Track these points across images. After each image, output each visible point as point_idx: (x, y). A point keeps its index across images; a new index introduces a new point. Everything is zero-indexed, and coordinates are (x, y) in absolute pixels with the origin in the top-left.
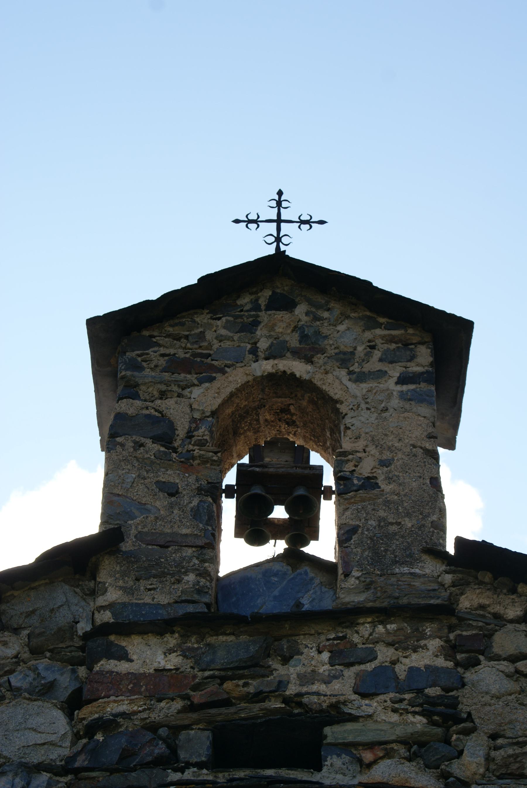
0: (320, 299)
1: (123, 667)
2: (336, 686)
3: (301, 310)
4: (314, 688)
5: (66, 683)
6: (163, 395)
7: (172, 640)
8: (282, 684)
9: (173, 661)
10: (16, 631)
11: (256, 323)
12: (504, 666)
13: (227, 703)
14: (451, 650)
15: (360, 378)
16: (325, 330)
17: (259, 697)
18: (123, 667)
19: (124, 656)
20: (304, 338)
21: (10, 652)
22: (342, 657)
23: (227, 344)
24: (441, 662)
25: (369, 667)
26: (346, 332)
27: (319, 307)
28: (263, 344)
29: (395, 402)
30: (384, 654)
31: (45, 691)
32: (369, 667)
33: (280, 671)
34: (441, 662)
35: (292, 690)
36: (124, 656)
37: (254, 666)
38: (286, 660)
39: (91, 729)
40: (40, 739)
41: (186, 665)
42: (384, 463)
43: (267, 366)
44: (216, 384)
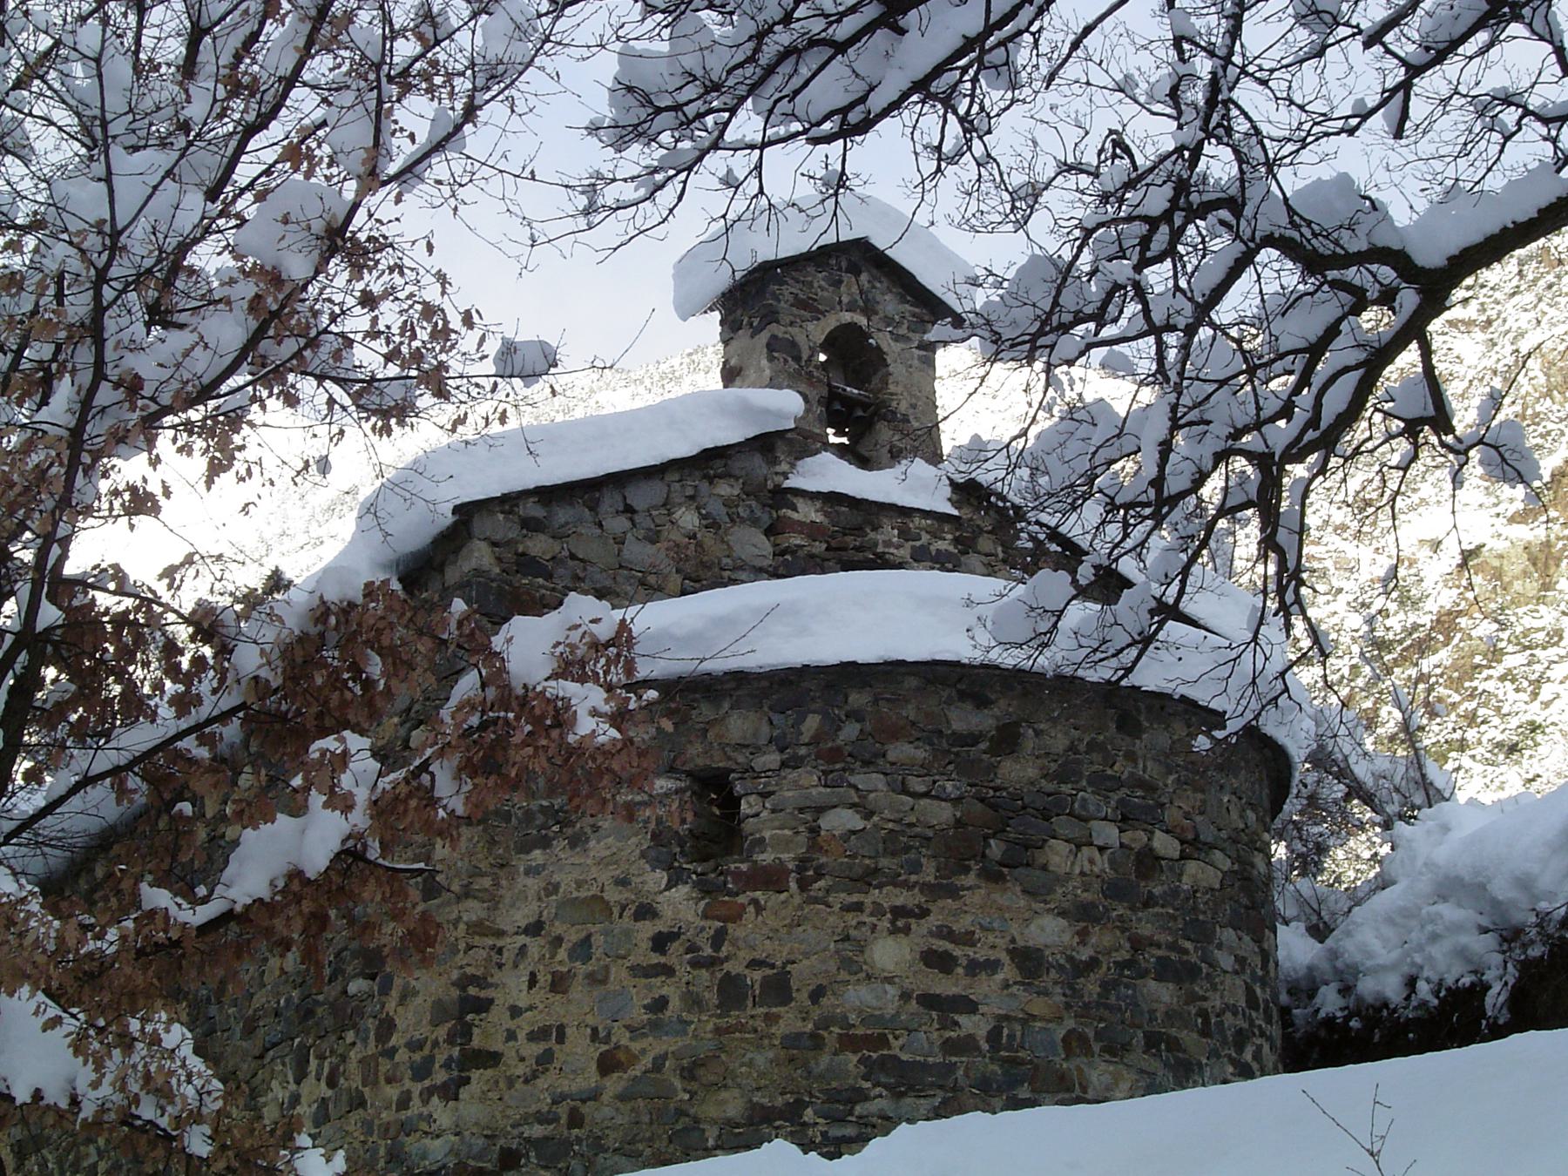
0: (875, 271)
1: (790, 513)
2: (902, 552)
3: (864, 277)
4: (892, 550)
5: (766, 520)
6: (791, 324)
7: (818, 504)
8: (876, 545)
9: (818, 518)
10: (737, 479)
11: (841, 282)
12: (983, 558)
13: (845, 549)
14: (956, 541)
15: (897, 338)
16: (879, 298)
17: (858, 549)
18: (795, 516)
19: (795, 509)
20: (866, 301)
21: (736, 492)
22: (905, 534)
23: (826, 294)
24: (951, 548)
25: (918, 544)
26: (890, 304)
27: (875, 278)
28: (845, 299)
29: (916, 363)
30: (925, 538)
31: (755, 522)
32: (918, 544)
33: (872, 535)
34: (951, 548)
35: (880, 549)
36: (795, 509)
37: (858, 530)
38: (875, 529)
39: (783, 553)
40: (757, 552)
41: (826, 521)
42: (914, 406)
43: (847, 317)
44: (823, 322)
